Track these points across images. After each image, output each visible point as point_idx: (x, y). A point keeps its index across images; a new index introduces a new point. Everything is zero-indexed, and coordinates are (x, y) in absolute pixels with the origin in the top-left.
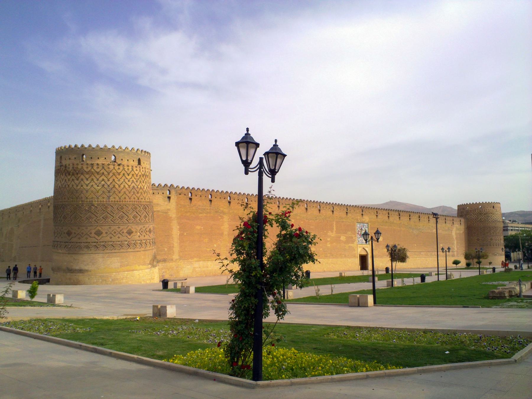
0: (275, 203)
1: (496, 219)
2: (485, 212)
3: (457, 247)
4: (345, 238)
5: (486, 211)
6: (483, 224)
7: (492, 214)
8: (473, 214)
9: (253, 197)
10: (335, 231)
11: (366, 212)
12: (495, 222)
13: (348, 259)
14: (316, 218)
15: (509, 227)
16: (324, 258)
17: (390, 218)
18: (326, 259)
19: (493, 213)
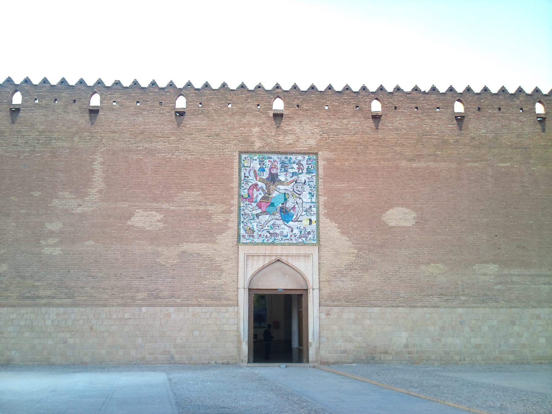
4: (159, 217)
10: (100, 192)
11: (305, 107)
13: (171, 309)
16: (14, 306)
18: (23, 310)
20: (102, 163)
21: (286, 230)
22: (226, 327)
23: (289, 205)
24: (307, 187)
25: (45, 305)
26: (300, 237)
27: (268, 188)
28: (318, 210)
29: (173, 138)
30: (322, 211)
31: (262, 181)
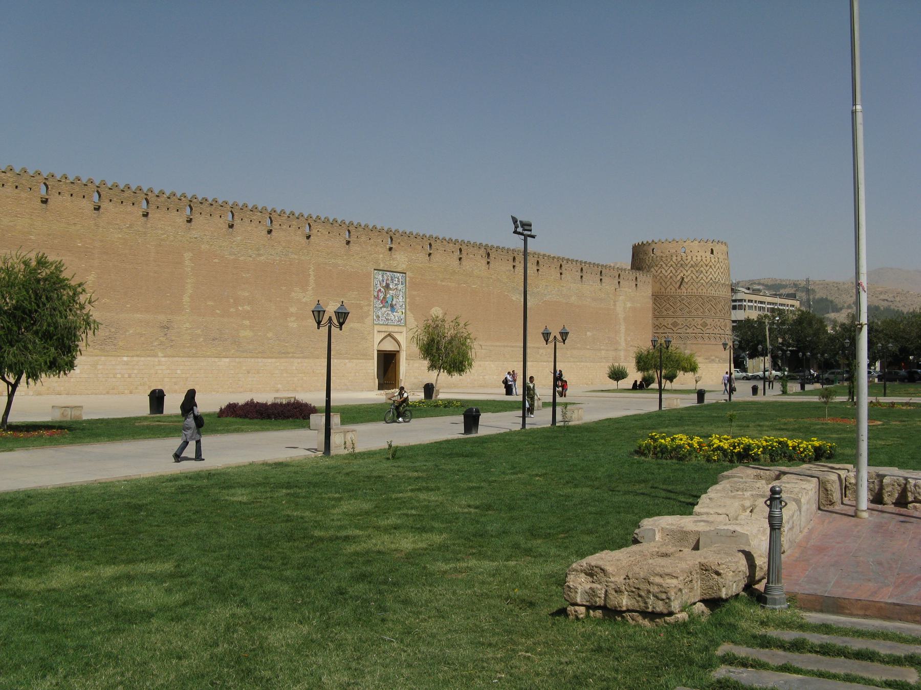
0: (133, 204)
1: (717, 280)
2: (692, 262)
3: (626, 340)
5: (694, 259)
6: (687, 290)
7: (708, 267)
8: (666, 266)
9: (66, 183)
11: (402, 244)
12: (714, 285)
13: (347, 361)
14: (258, 249)
15: (745, 301)
16: (276, 358)
17: (464, 262)
18: (283, 360)
19: (711, 264)
20: (313, 271)
21: (393, 318)
22: (369, 371)
23: (394, 303)
24: (401, 292)
25: (291, 357)
26: (398, 321)
27: (385, 292)
28: (405, 306)
29: (345, 257)
30: (408, 307)
31: (383, 287)
